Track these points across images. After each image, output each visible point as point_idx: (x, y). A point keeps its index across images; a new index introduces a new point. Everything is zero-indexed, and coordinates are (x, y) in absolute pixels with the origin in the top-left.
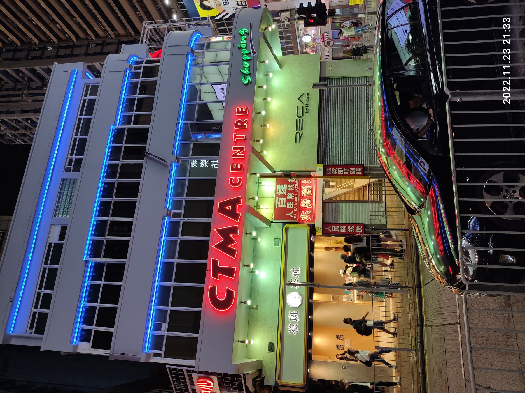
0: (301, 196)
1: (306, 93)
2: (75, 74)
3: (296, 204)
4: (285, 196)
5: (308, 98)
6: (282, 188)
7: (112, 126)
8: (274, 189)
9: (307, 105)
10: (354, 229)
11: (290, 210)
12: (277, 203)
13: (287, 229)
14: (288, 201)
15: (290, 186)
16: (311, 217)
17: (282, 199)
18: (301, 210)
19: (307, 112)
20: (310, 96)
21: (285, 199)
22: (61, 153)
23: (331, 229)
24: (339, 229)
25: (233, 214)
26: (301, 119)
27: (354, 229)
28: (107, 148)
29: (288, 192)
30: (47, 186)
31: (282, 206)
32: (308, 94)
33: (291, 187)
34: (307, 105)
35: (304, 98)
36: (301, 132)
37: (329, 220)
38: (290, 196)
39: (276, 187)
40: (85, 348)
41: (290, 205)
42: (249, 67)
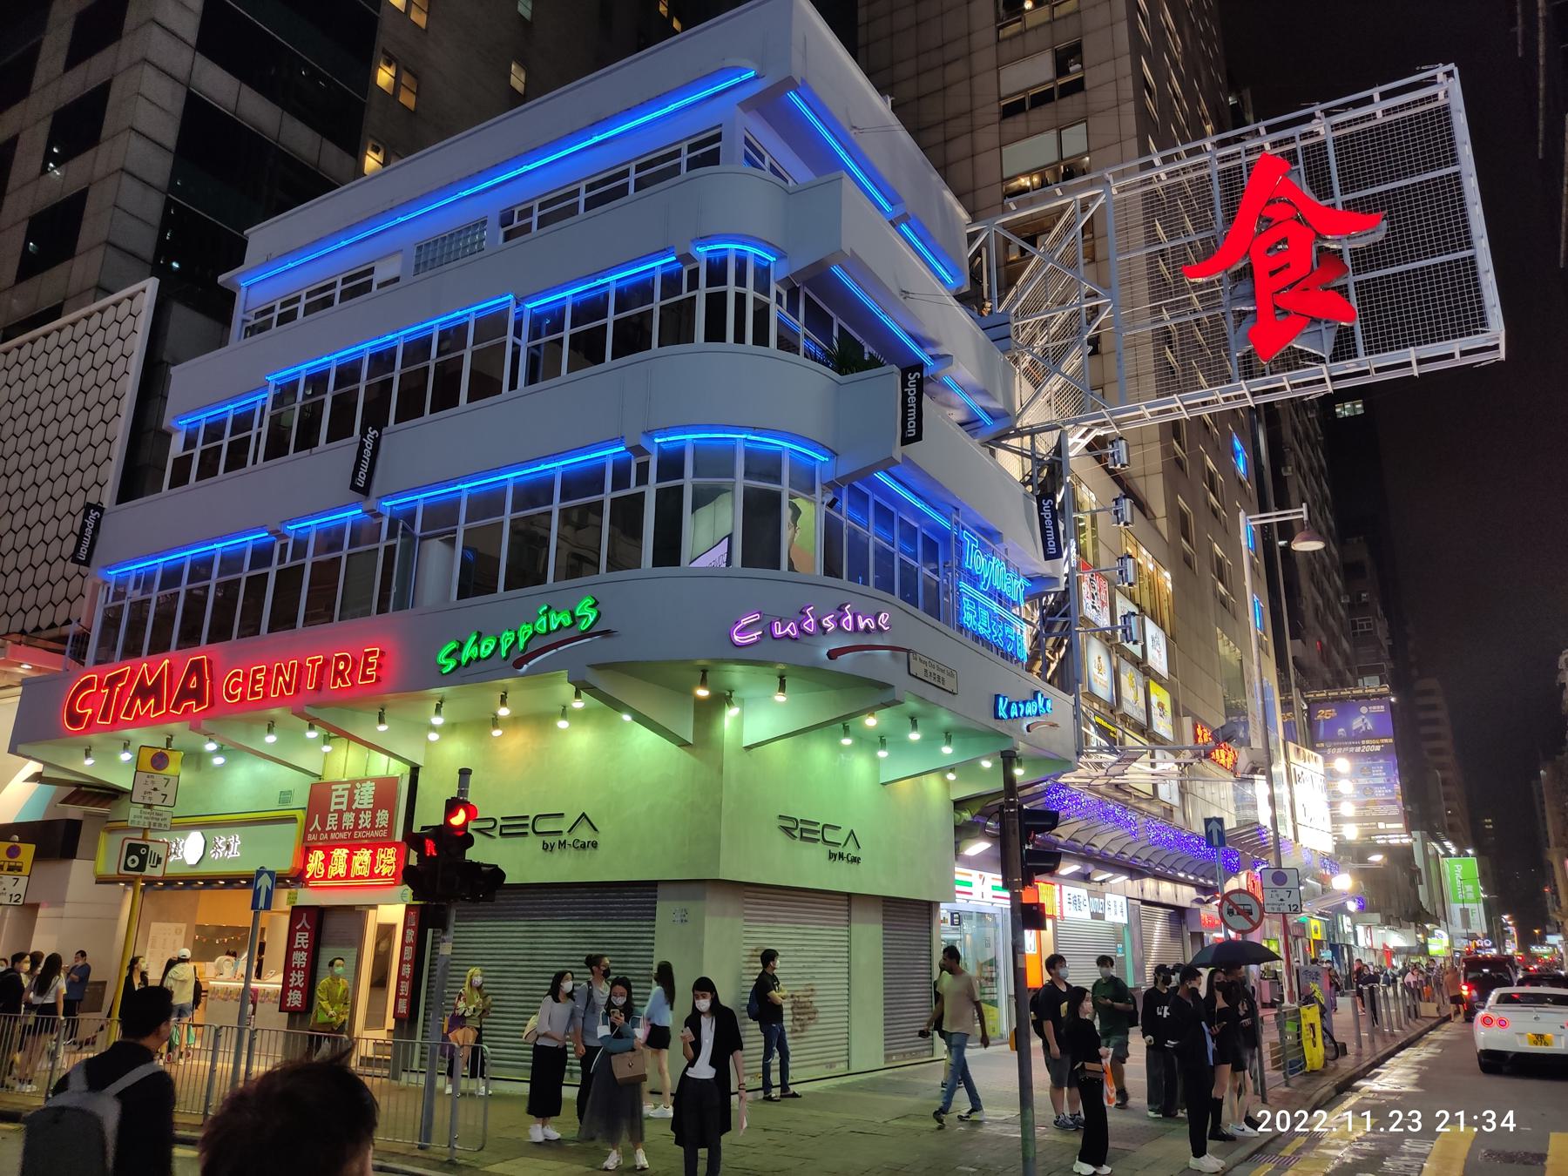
0: (353, 848)
1: (600, 839)
2: (737, 80)
3: (333, 836)
4: (349, 809)
5: (584, 846)
6: (365, 797)
7: (510, 297)
8: (340, 777)
9: (562, 844)
10: (297, 988)
11: (323, 823)
12: (340, 787)
13: (293, 820)
14: (340, 813)
15: (368, 816)
16: (312, 878)
17: (345, 800)
18: (328, 850)
19: (546, 847)
20: (588, 852)
21: (344, 807)
22: (539, 173)
23: (303, 929)
24: (301, 949)
25: (186, 694)
26: (529, 830)
27: (297, 988)
28: (458, 314)
29: (358, 811)
30: (465, 194)
31: (334, 800)
32: (595, 845)
33: (365, 818)
34: (562, 844)
35: (584, 834)
36: (496, 833)
37: (332, 924)
38: (348, 819)
39: (372, 780)
40: (176, 448)
41: (332, 821)
42: (479, 658)
